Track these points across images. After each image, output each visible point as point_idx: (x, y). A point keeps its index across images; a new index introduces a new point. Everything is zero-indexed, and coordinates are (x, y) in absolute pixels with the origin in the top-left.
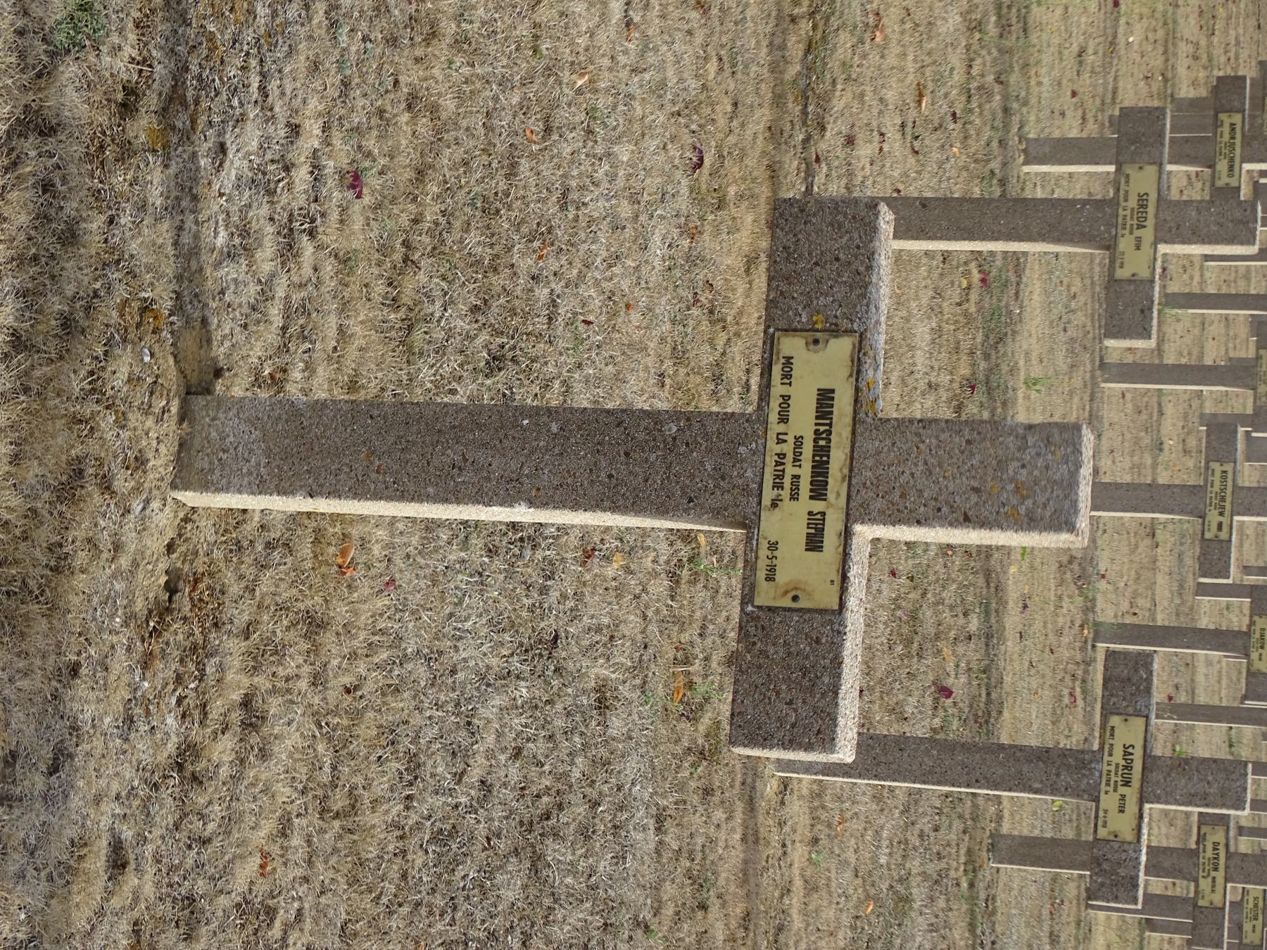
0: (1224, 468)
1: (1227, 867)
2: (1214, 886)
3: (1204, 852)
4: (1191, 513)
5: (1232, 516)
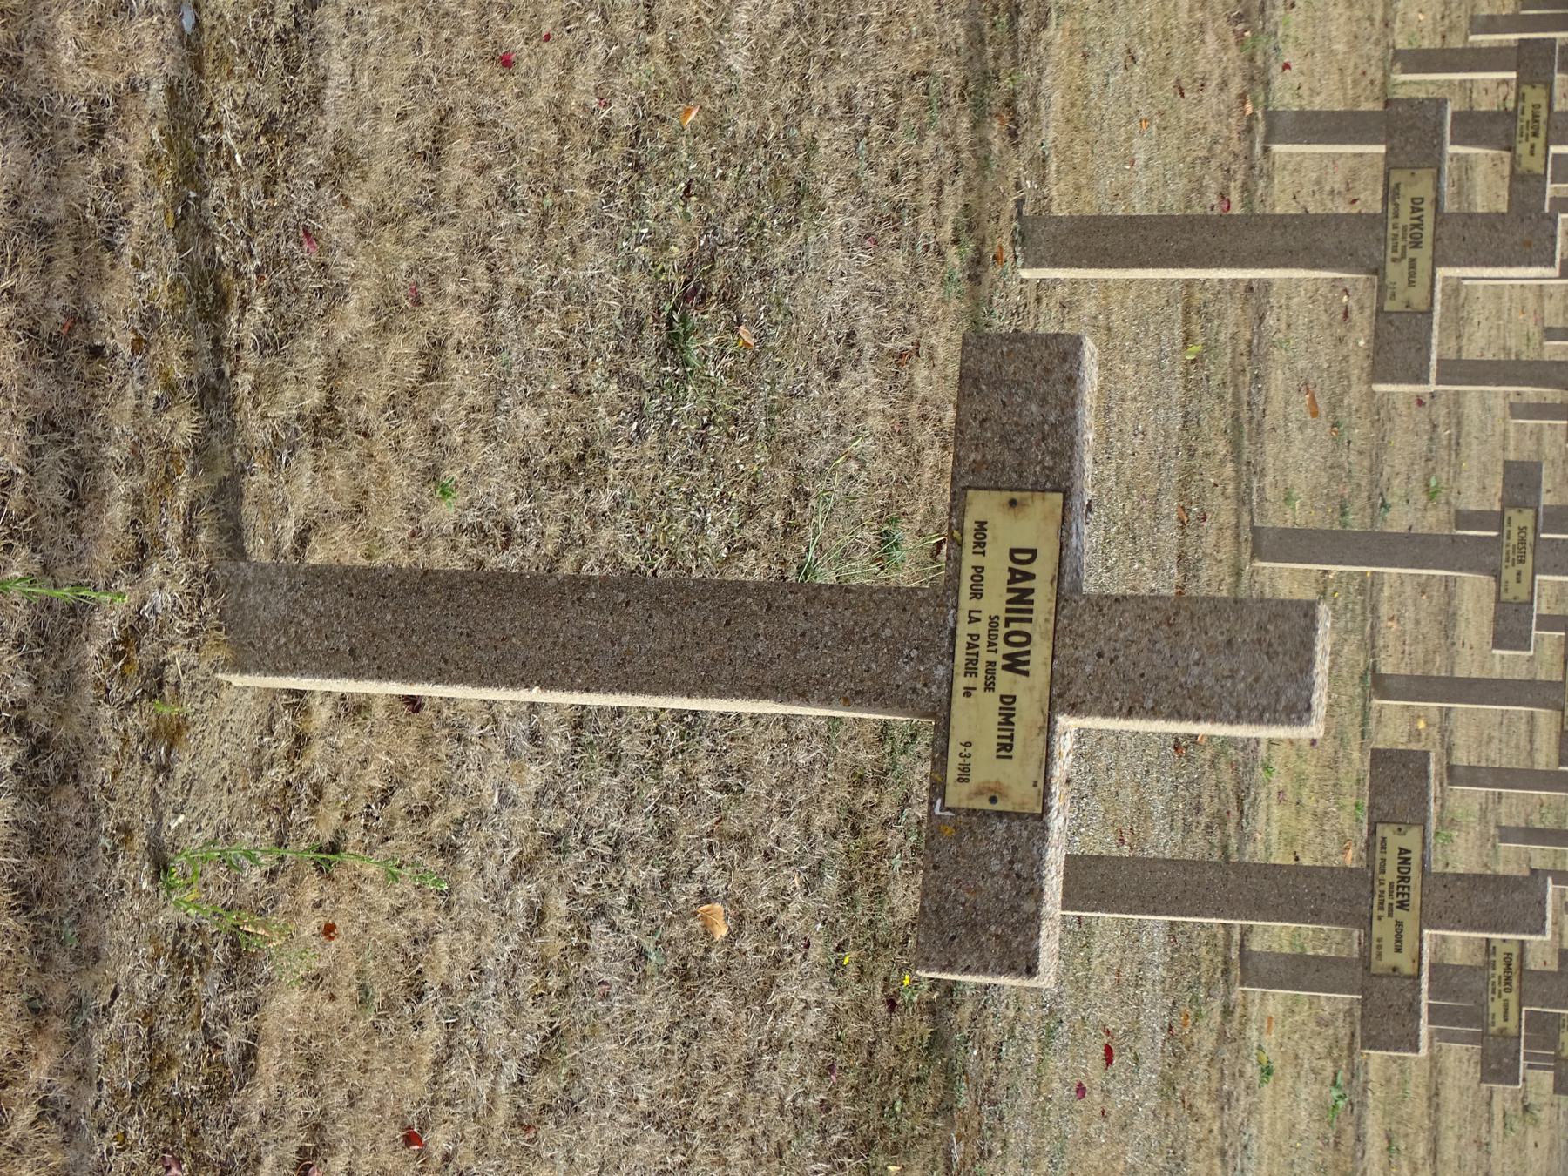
1: (1436, 239)
2: (1412, 275)
3: (1396, 216)
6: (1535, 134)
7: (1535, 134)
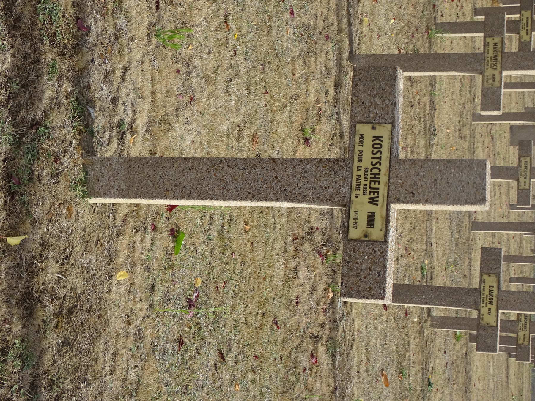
0: (377, 133)
4: (329, 200)
5: (388, 205)
6: (491, 303)
7: (491, 303)
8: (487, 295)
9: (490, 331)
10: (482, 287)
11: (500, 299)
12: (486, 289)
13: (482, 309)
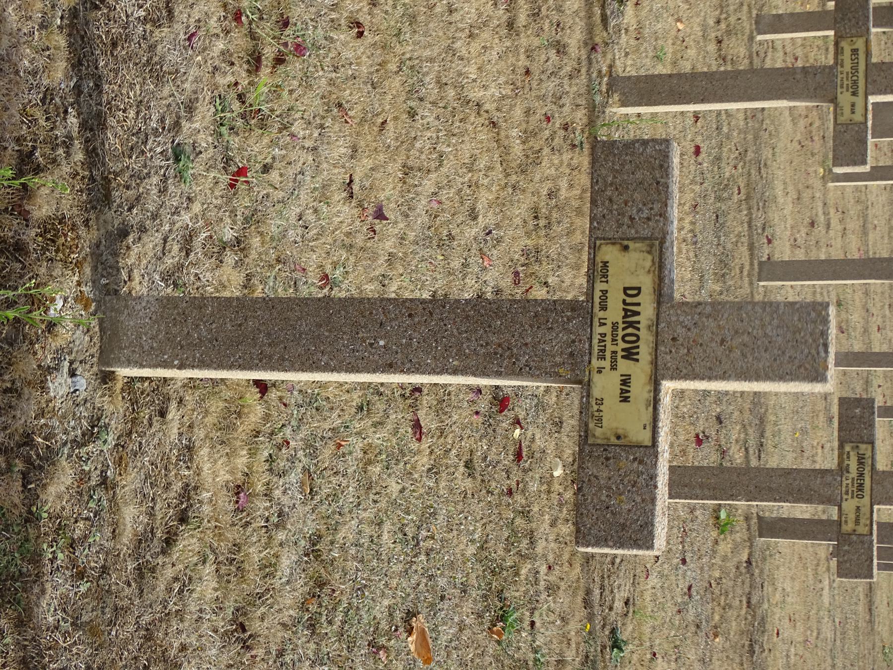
6: (630, 355)
7: (630, 355)
8: (615, 326)
9: (626, 462)
10: (597, 294)
11: (667, 336)
12: (610, 303)
13: (596, 378)
